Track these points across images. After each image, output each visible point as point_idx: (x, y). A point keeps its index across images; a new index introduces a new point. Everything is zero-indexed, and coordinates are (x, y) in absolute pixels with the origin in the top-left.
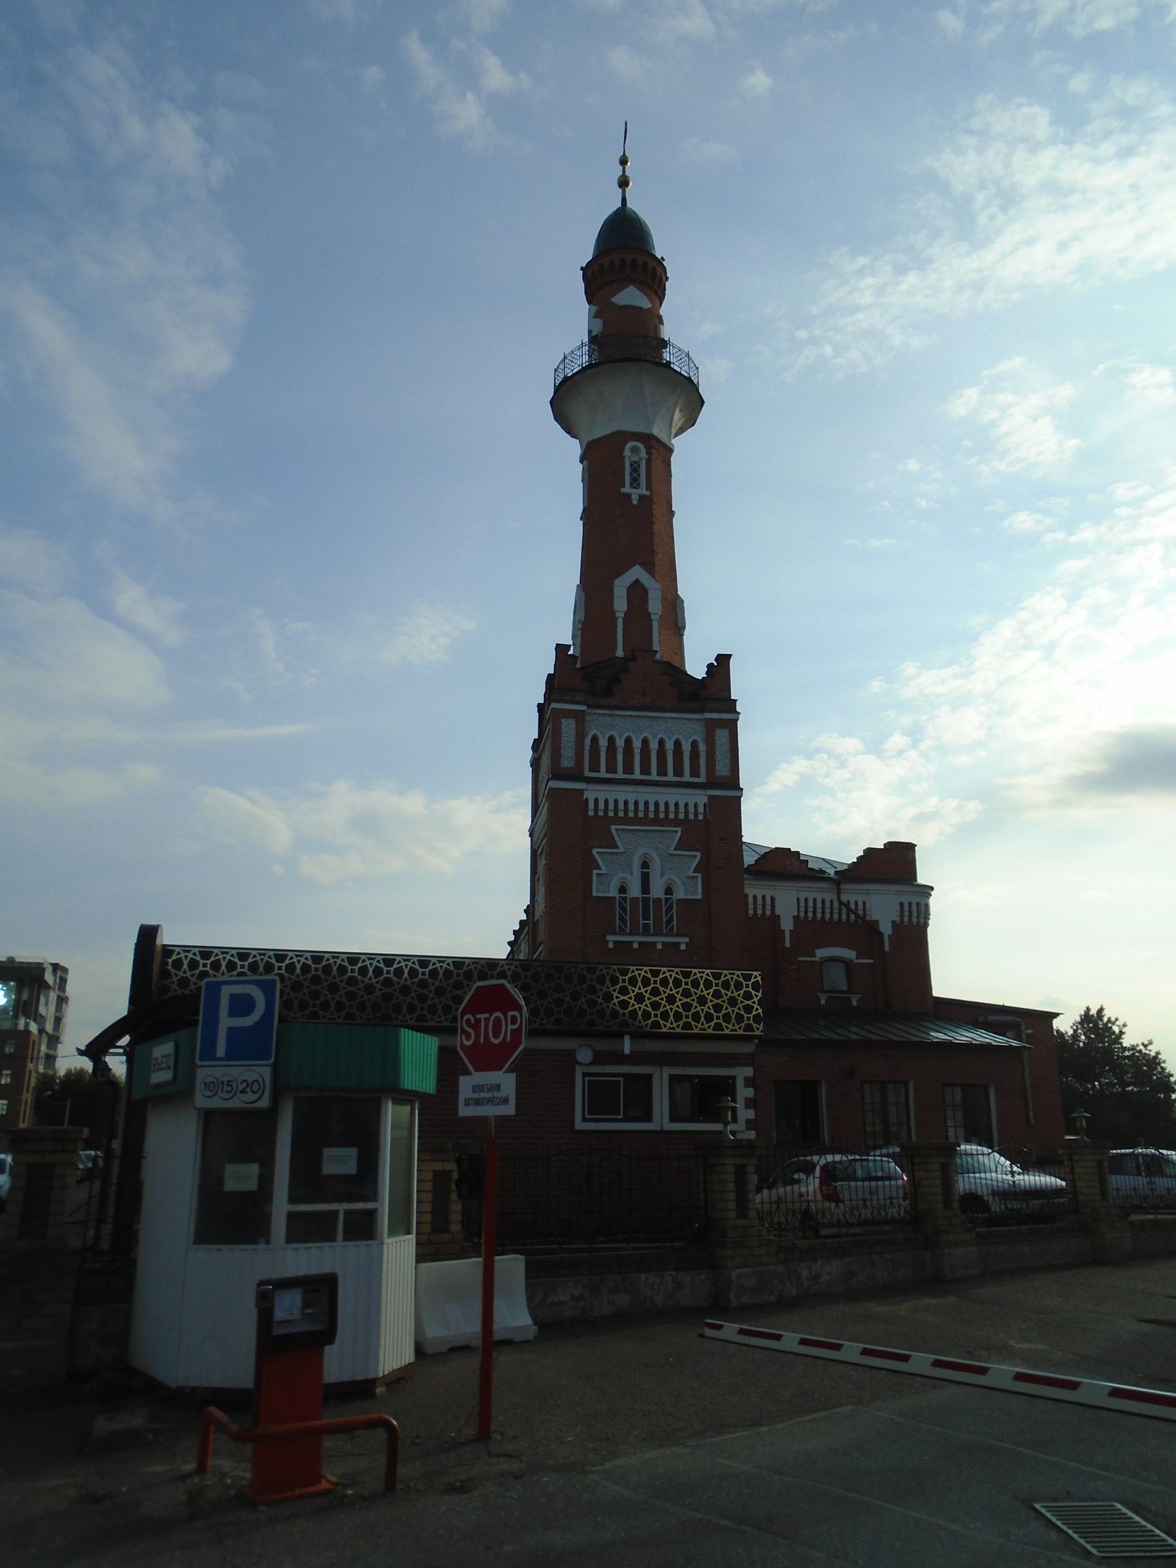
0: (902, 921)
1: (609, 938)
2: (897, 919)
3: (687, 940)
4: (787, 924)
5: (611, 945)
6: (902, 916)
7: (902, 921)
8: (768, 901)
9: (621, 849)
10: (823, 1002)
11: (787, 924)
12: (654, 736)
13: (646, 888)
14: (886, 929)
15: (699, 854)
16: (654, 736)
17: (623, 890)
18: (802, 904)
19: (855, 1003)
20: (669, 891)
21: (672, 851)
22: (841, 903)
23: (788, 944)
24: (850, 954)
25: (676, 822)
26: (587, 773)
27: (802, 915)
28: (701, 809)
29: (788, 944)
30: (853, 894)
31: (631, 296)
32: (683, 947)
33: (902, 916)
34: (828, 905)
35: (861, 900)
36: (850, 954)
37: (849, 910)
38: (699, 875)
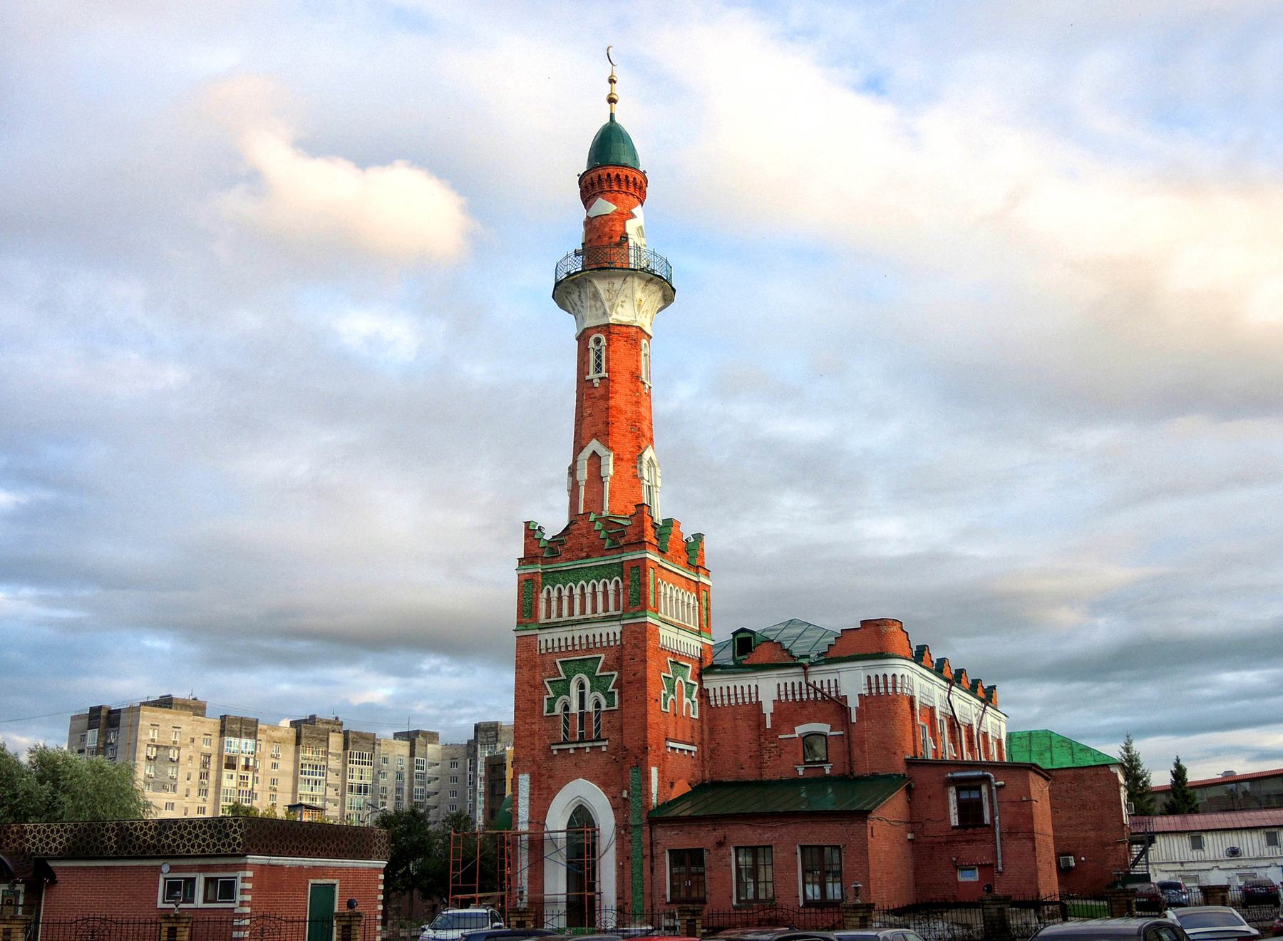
0: (870, 693)
2: (865, 692)
4: (768, 708)
6: (870, 689)
7: (870, 693)
8: (753, 690)
9: (564, 677)
10: (801, 773)
11: (768, 708)
12: (588, 583)
13: (582, 705)
14: (853, 703)
15: (616, 673)
16: (588, 583)
17: (566, 708)
18: (782, 688)
19: (828, 772)
20: (598, 705)
22: (808, 685)
23: (769, 726)
24: (824, 728)
25: (603, 649)
27: (783, 698)
28: (618, 637)
29: (769, 726)
30: (820, 676)
31: (604, 206)
32: (604, 749)
33: (870, 689)
34: (797, 687)
35: (832, 677)
36: (824, 728)
37: (816, 689)
38: (616, 691)
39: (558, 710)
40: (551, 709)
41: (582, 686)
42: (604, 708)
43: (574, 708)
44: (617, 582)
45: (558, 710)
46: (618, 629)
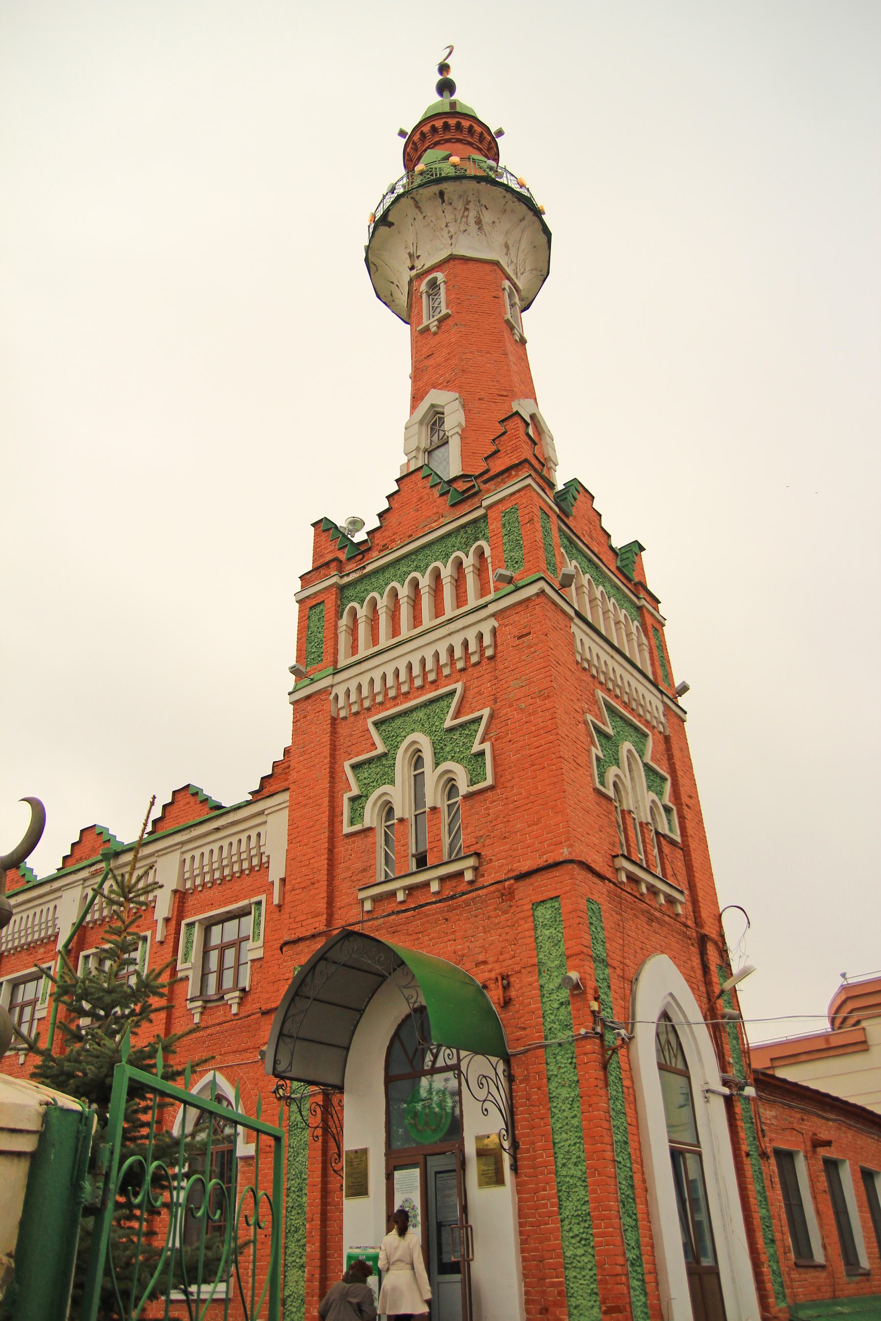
1: (361, 895)
3: (471, 862)
5: (368, 906)
9: (381, 749)
20: (451, 789)
21: (448, 723)
26: (341, 664)
28: (487, 640)
32: (469, 876)
38: (487, 746)
39: (370, 817)
40: (356, 816)
41: (418, 762)
42: (463, 788)
43: (403, 808)
44: (481, 554)
45: (370, 817)
46: (486, 628)
